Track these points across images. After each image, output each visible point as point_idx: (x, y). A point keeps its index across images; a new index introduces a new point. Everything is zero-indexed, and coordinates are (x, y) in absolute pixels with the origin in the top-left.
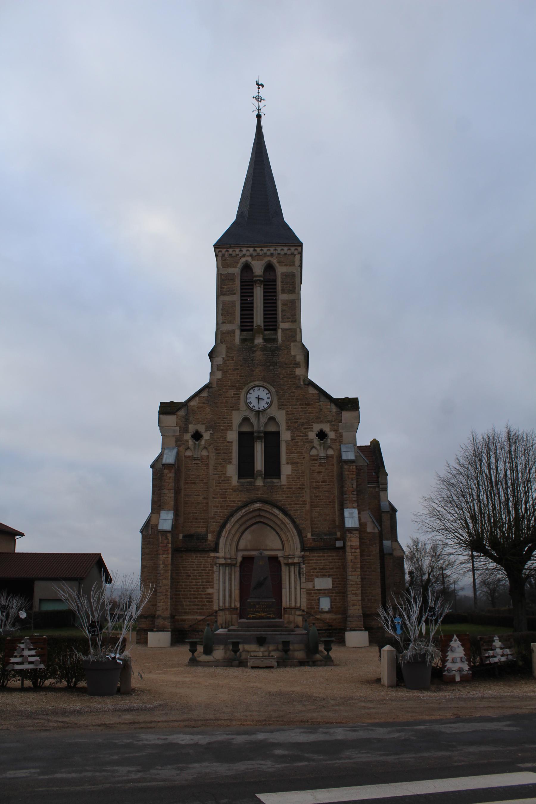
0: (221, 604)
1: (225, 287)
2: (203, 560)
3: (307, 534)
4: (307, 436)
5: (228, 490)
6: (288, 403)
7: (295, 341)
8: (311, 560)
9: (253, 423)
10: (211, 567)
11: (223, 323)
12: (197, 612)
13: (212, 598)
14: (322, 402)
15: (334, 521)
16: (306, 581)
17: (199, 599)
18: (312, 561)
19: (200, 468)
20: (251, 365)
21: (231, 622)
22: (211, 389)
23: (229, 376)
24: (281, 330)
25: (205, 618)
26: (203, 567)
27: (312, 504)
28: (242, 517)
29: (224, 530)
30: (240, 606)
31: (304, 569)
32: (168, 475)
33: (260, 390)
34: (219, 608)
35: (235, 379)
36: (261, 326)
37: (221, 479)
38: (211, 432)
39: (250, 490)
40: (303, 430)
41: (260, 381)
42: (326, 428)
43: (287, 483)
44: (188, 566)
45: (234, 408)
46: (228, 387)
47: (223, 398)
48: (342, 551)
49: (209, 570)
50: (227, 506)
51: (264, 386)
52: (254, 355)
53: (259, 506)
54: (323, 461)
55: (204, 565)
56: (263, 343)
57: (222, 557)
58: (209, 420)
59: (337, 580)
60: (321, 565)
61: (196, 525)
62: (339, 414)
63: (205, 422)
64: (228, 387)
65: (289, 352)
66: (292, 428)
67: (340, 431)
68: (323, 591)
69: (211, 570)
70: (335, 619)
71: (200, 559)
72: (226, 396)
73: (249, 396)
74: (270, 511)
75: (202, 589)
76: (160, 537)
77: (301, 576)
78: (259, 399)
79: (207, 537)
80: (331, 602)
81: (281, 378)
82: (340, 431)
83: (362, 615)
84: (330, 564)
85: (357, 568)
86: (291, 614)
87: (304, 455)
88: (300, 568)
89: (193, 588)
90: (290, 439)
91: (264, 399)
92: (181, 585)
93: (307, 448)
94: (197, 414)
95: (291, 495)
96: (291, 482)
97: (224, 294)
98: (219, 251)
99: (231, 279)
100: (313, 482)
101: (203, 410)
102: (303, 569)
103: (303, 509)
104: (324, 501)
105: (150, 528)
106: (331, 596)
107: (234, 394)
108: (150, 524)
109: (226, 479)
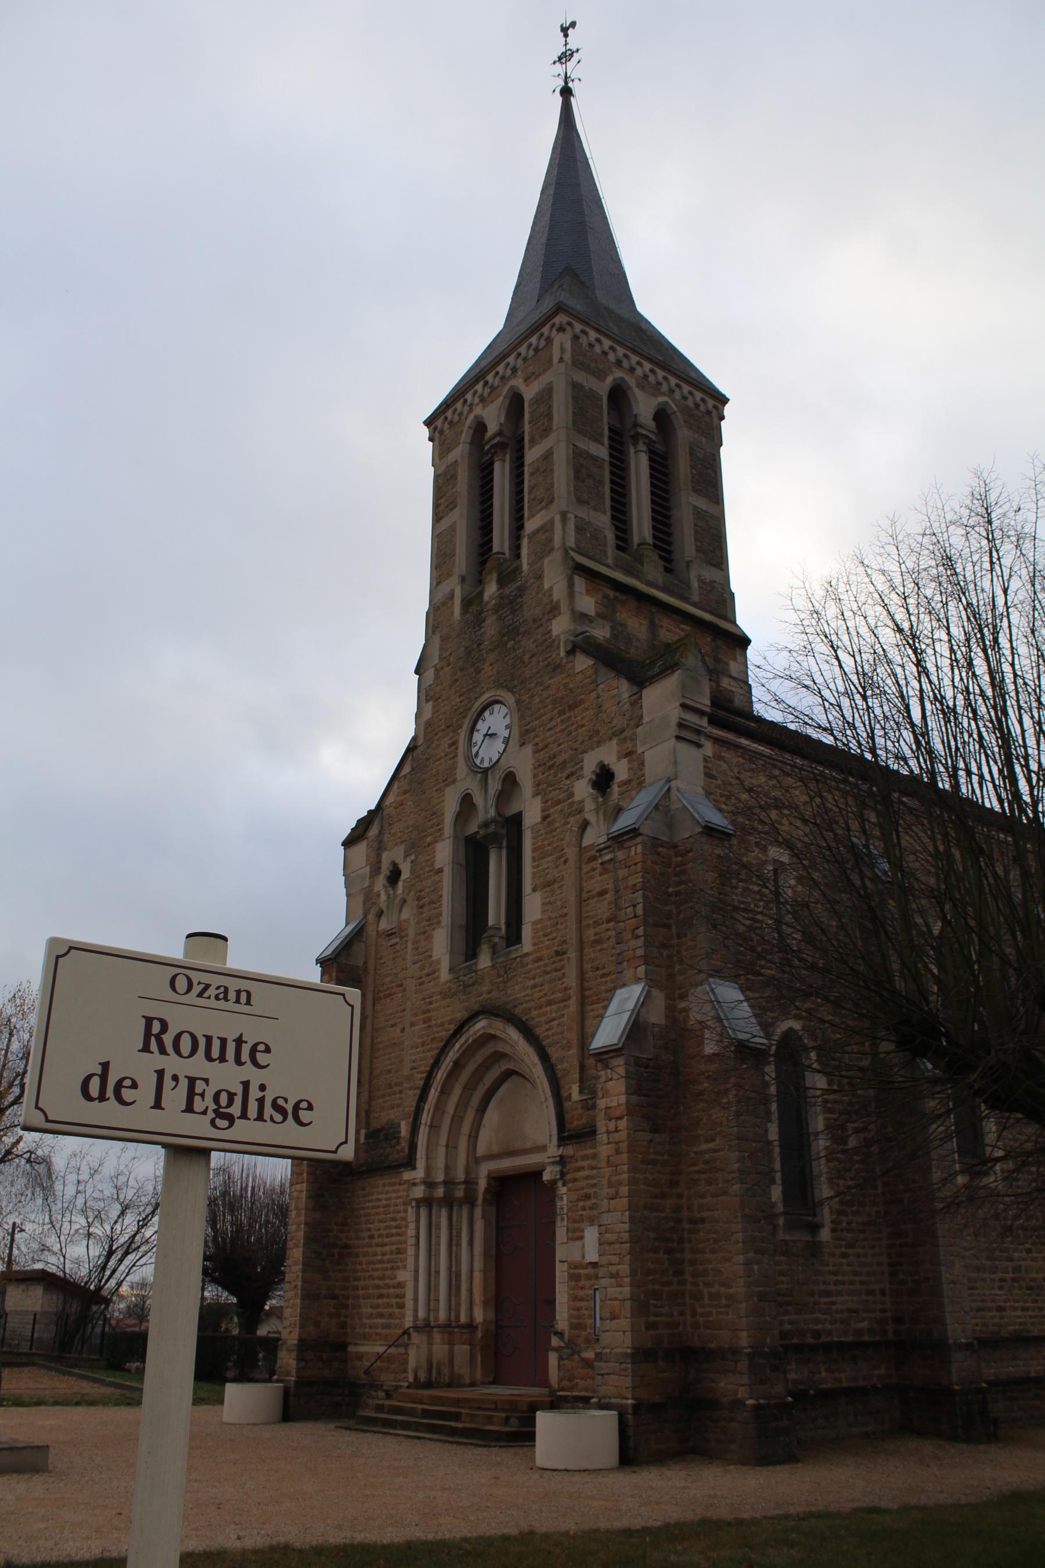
0: (421, 1314)
3: (570, 1088)
4: (571, 795)
8: (579, 1169)
11: (439, 583)
16: (568, 1238)
18: (582, 1174)
22: (415, 753)
25: (385, 1352)
28: (458, 1065)
31: (565, 1197)
36: (504, 554)
38: (413, 857)
42: (608, 754)
51: (497, 698)
52: (482, 630)
53: (484, 1027)
54: (608, 857)
56: (498, 590)
62: (636, 701)
65: (540, 587)
67: (639, 751)
79: (400, 1132)
81: (526, 660)
82: (639, 751)
85: (620, 1183)
87: (566, 853)
89: (377, 1270)
90: (539, 820)
91: (496, 734)
92: (361, 1264)
95: (541, 980)
102: (562, 1199)
103: (563, 1015)
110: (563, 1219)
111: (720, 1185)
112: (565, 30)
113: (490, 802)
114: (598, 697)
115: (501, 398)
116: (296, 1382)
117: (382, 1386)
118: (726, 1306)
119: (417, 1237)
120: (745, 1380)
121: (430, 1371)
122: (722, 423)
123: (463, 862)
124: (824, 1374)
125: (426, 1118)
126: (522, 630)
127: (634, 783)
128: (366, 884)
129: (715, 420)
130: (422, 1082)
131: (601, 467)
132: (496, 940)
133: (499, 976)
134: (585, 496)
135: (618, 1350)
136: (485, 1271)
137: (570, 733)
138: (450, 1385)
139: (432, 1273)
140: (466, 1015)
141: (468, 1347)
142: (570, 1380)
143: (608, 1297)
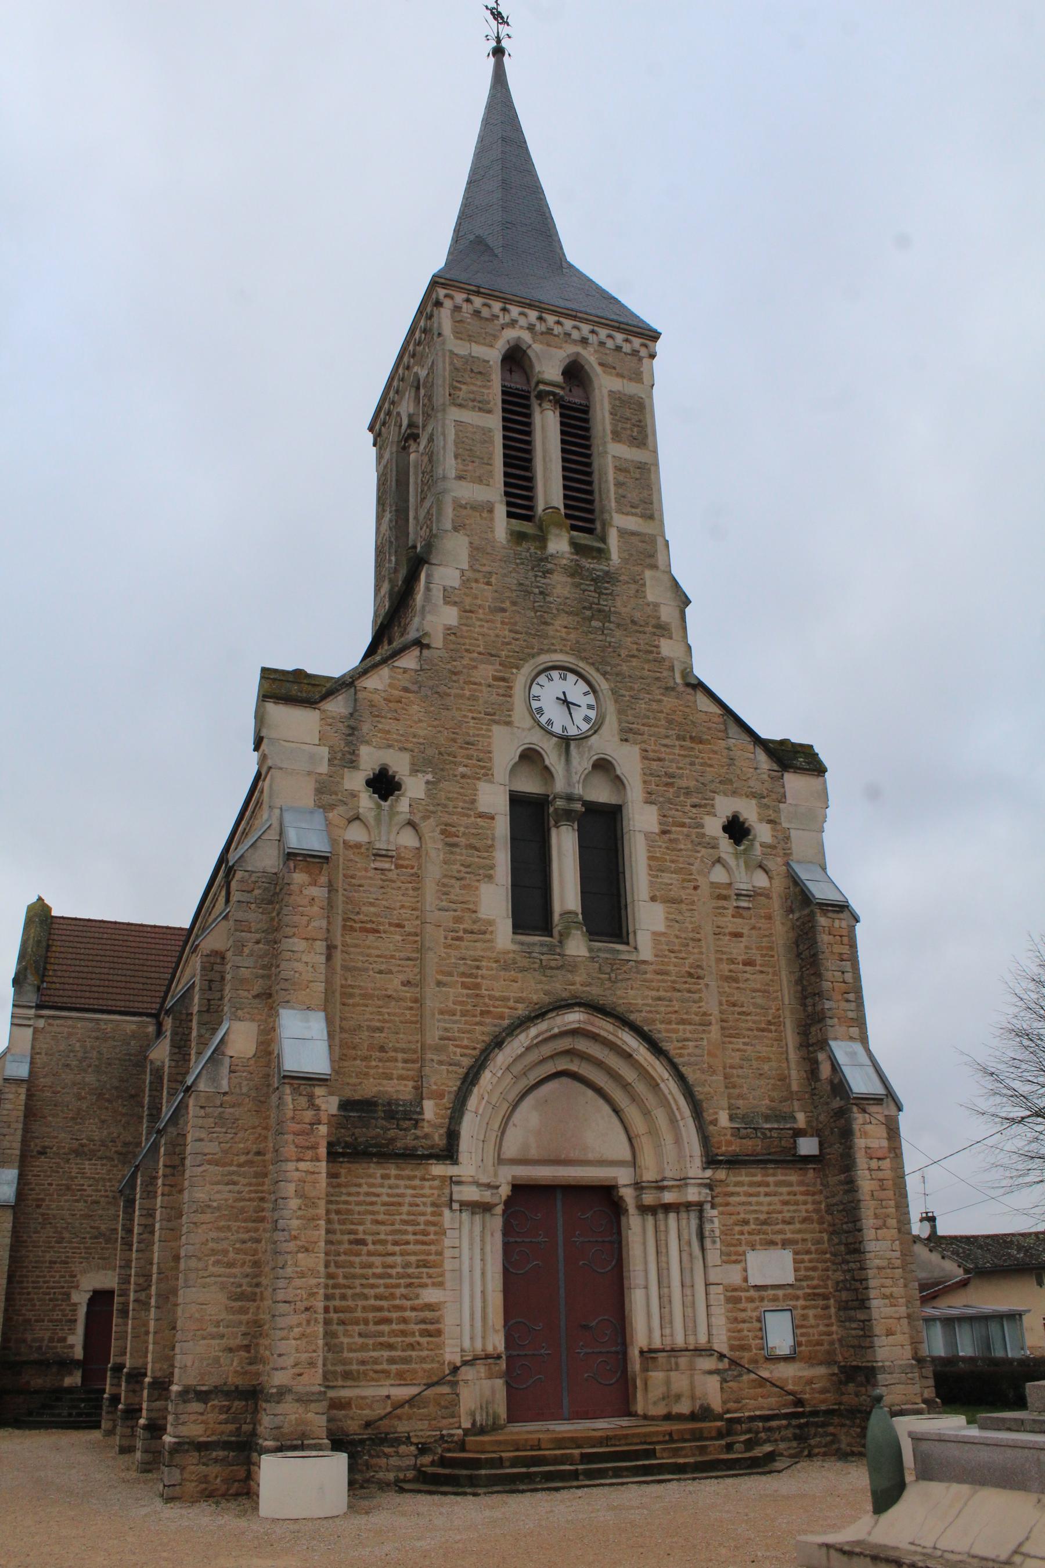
1: (464, 387)
2: (406, 1187)
3: (716, 1113)
4: (702, 826)
5: (484, 963)
6: (646, 728)
7: (654, 567)
8: (732, 1194)
9: (553, 769)
10: (433, 1214)
11: (460, 478)
12: (386, 1373)
13: (438, 1321)
14: (733, 741)
15: (783, 1078)
17: (394, 1327)
19: (393, 885)
20: (541, 606)
22: (425, 652)
23: (478, 623)
24: (619, 531)
25: (419, 1394)
26: (409, 1213)
27: (725, 1024)
29: (476, 1090)
30: (507, 1348)
31: (716, 1220)
32: (306, 892)
33: (565, 679)
34: (462, 1356)
35: (497, 636)
37: (462, 926)
38: (429, 777)
39: (552, 968)
40: (688, 808)
41: (567, 653)
42: (749, 812)
43: (656, 956)
44: (357, 1208)
45: (496, 718)
47: (465, 683)
48: (814, 1169)
49: (428, 1223)
50: (482, 1013)
53: (579, 1022)
54: (745, 904)
55: (411, 1205)
57: (470, 1179)
58: (422, 740)
59: (806, 1257)
60: (762, 1212)
61: (381, 1071)
63: (410, 746)
64: (476, 655)
65: (640, 593)
66: (661, 799)
67: (785, 825)
68: (771, 1292)
69: (434, 1224)
70: (810, 1382)
71: (397, 1187)
72: (472, 679)
73: (536, 690)
74: (611, 1037)
75: (403, 1290)
76: (288, 1099)
77: (708, 1243)
78: (565, 702)
79: (421, 1113)
80: (795, 1327)
81: (623, 656)
82: (785, 825)
83: (914, 1362)
84: (786, 1208)
86: (677, 1370)
88: (701, 1218)
89: (373, 1286)
90: (657, 831)
93: (702, 861)
94: (385, 718)
95: (669, 994)
96: (666, 956)
97: (460, 406)
98: (446, 296)
99: (480, 373)
100: (721, 959)
101: (403, 709)
102: (712, 1222)
104: (754, 1018)
105: (225, 1070)
106: (795, 1307)
107: (495, 678)
108: (223, 1054)
109: (475, 927)
110: (714, 1242)
117: (408, 1438)
131: (620, 498)
137: (692, 764)
142: (737, 1401)
143: (883, 1316)
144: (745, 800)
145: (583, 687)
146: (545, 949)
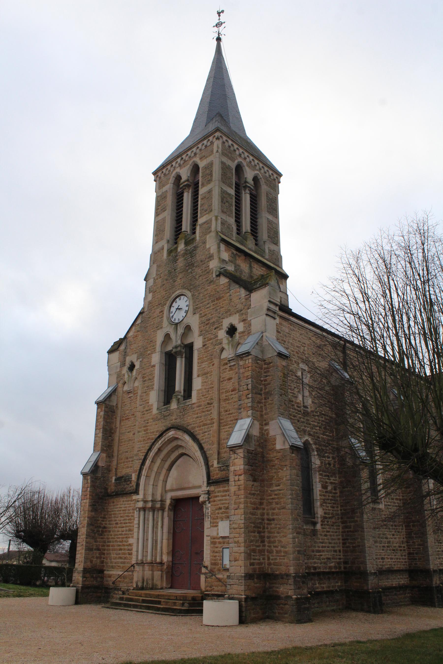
3: (213, 462)
4: (217, 336)
8: (216, 496)
11: (156, 242)
18: (218, 498)
21: (153, 580)
22: (143, 315)
28: (160, 450)
31: (210, 508)
36: (187, 232)
38: (141, 360)
42: (234, 320)
46: (155, 307)
53: (173, 434)
56: (185, 247)
62: (248, 298)
63: (137, 351)
67: (249, 319)
79: (131, 478)
81: (197, 278)
82: (249, 319)
89: (119, 538)
90: (201, 346)
92: (111, 535)
95: (200, 415)
102: (208, 509)
110: (208, 518)
111: (282, 505)
112: (219, 13)
113: (178, 337)
114: (230, 296)
115: (189, 166)
116: (82, 587)
117: (121, 589)
118: (284, 556)
119: (139, 524)
120: (292, 587)
121: (143, 582)
122: (280, 184)
123: (164, 363)
124: (317, 585)
125: (144, 472)
126: (195, 265)
127: (246, 333)
128: (118, 370)
129: (277, 183)
130: (143, 457)
131: (232, 198)
132: (179, 397)
133: (180, 412)
134: (225, 210)
135: (238, 574)
136: (168, 540)
137: (217, 310)
138: (152, 589)
139: (145, 540)
140: (164, 429)
141: (160, 572)
142: (210, 587)
143: (234, 551)
144: (234, 316)
145: (185, 298)
146: (165, 410)
